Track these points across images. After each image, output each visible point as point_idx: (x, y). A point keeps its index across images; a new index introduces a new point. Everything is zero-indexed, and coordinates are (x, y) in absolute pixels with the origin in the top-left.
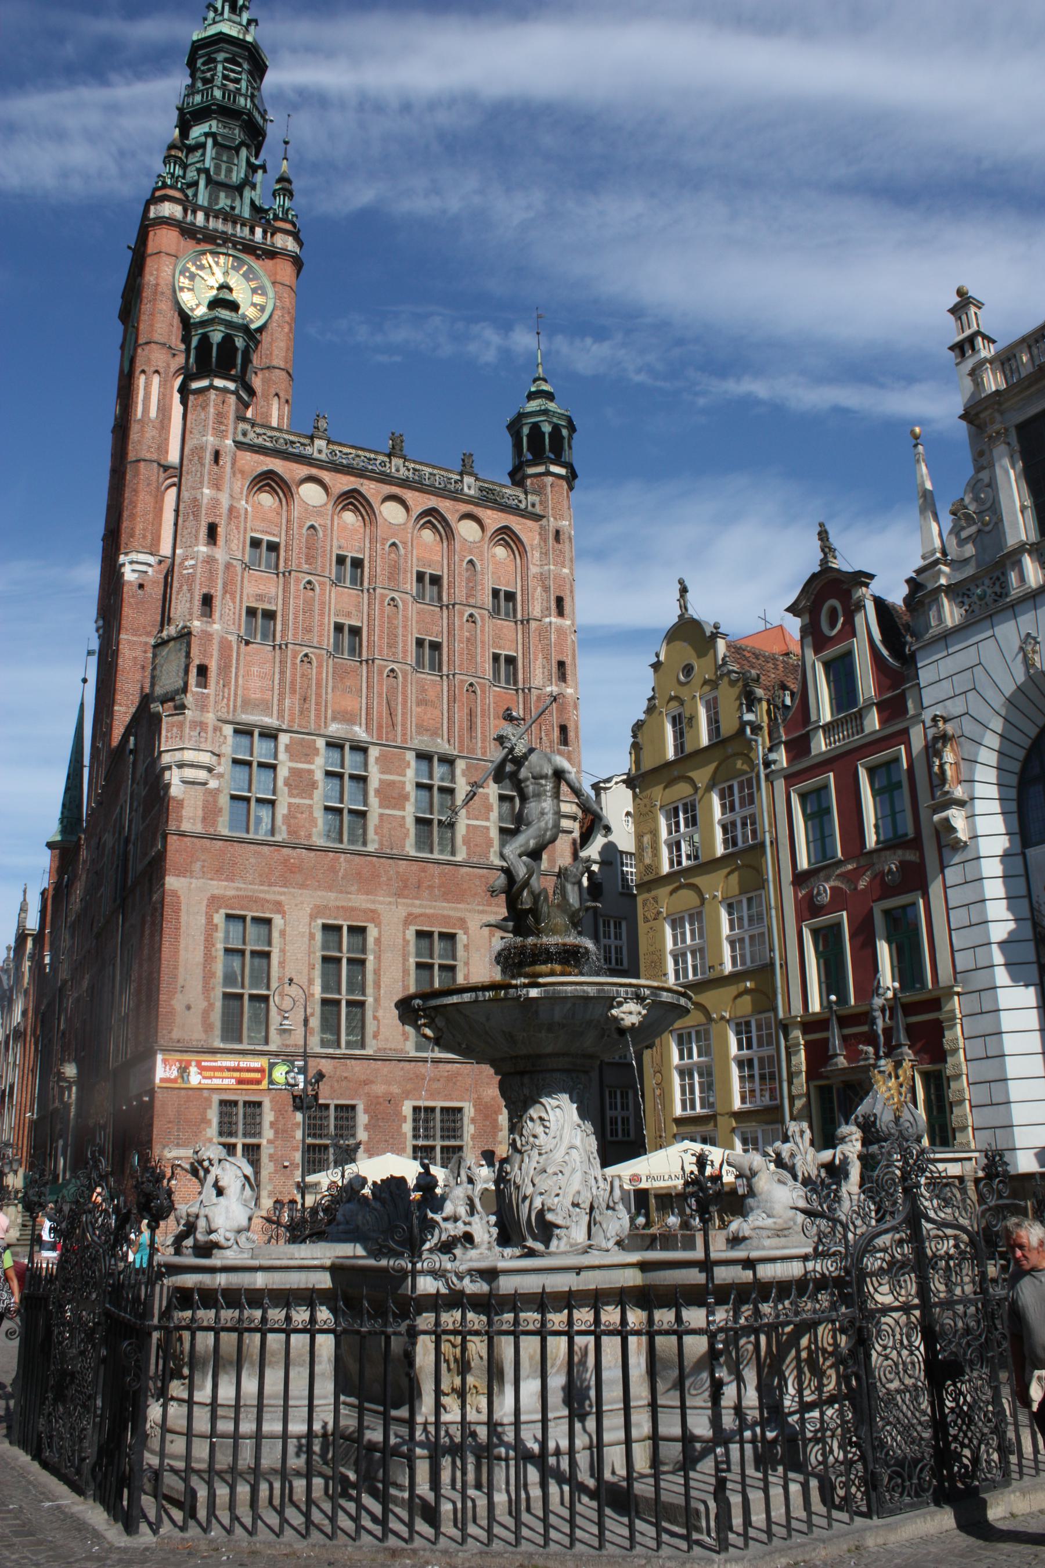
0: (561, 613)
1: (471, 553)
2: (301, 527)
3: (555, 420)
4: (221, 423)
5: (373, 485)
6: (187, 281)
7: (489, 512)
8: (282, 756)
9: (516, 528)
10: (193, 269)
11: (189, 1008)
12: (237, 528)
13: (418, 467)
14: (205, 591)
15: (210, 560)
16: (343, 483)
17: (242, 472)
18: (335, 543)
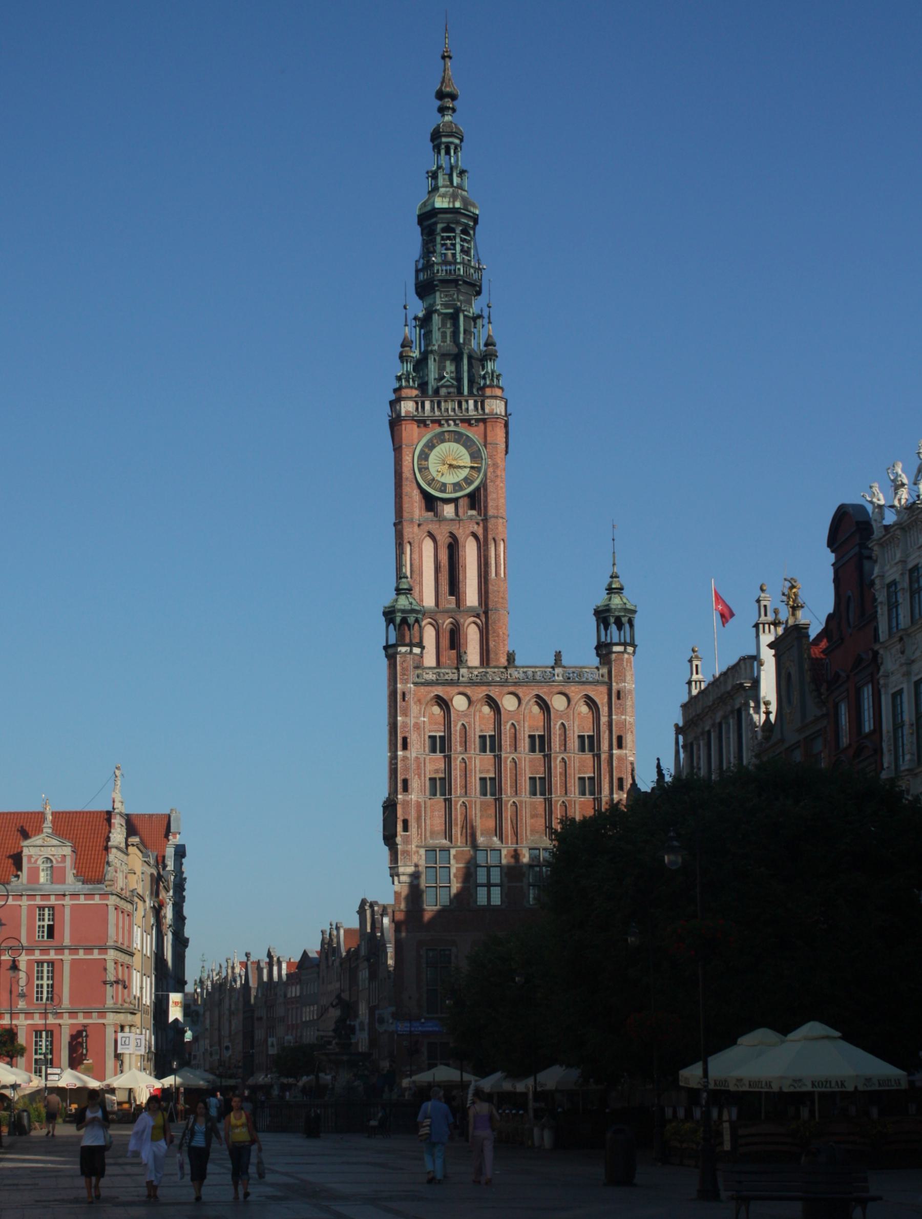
0: (620, 746)
1: (561, 718)
2: (456, 726)
3: (617, 614)
4: (404, 674)
5: (497, 689)
6: (423, 462)
7: (573, 688)
8: (452, 862)
9: (592, 694)
10: (426, 450)
11: (410, 998)
12: (419, 735)
13: (525, 670)
14: (403, 777)
15: (405, 758)
16: (479, 693)
17: (419, 701)
18: (477, 730)
